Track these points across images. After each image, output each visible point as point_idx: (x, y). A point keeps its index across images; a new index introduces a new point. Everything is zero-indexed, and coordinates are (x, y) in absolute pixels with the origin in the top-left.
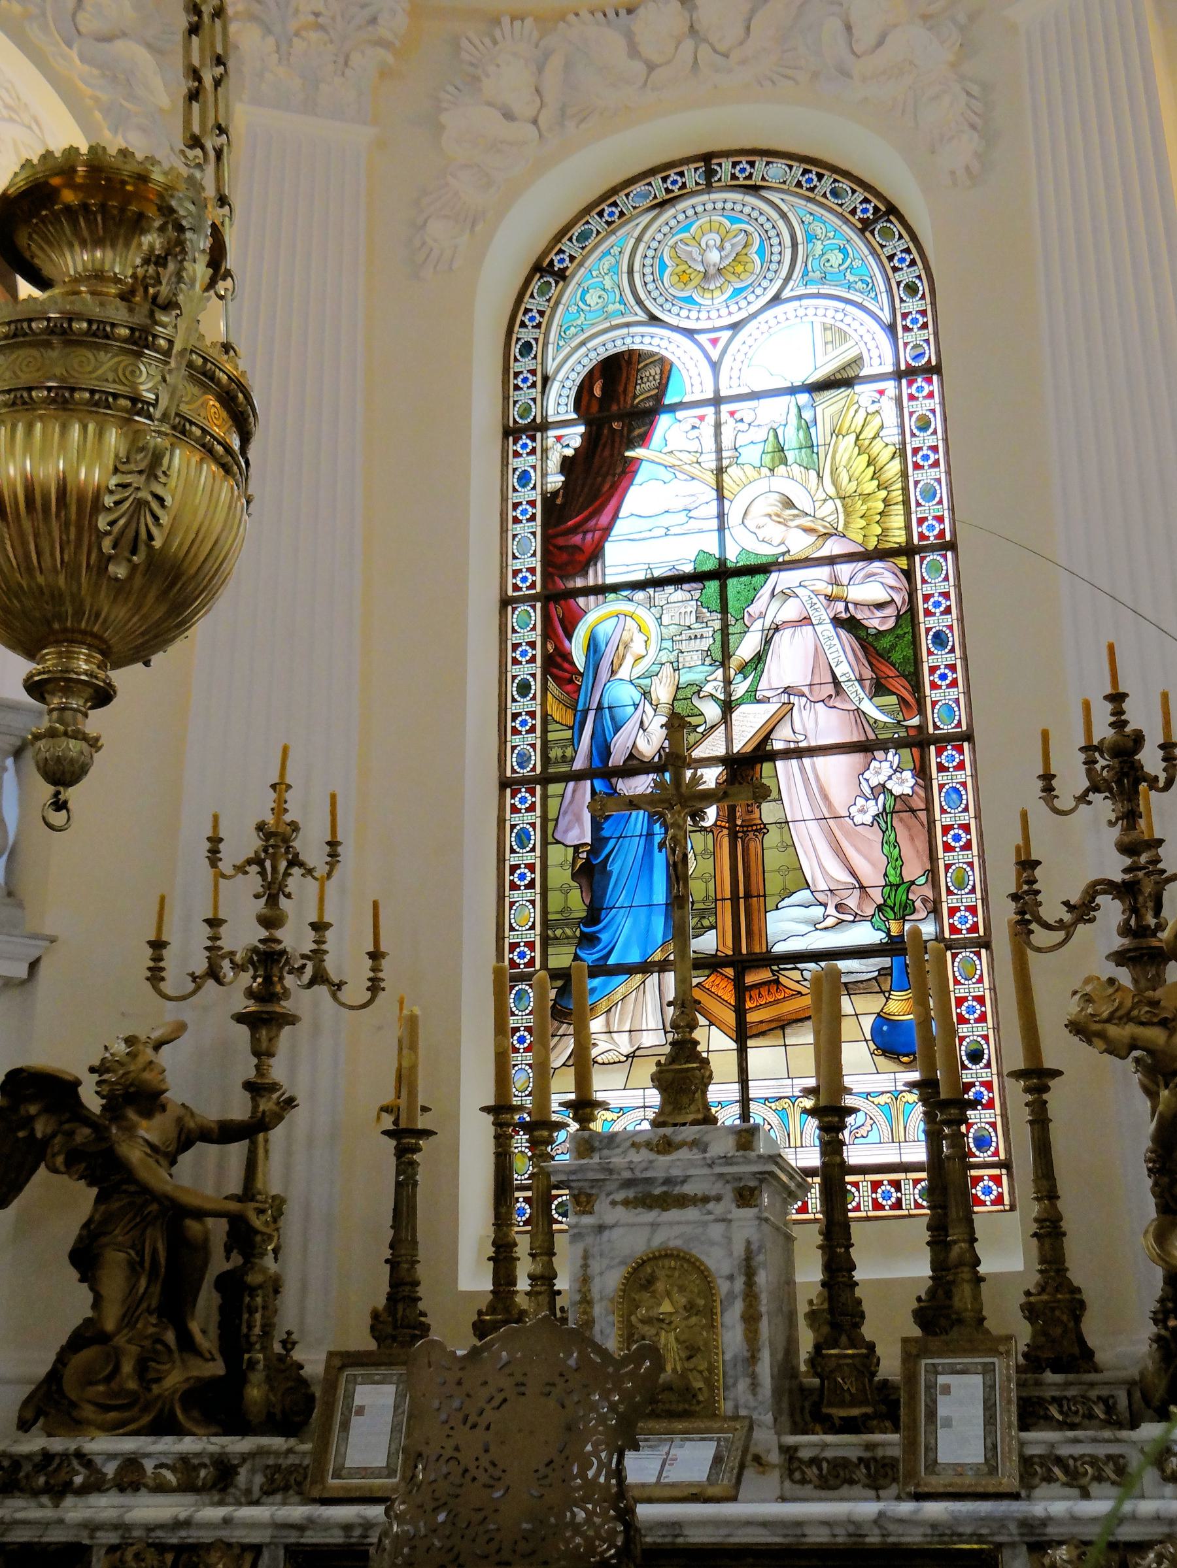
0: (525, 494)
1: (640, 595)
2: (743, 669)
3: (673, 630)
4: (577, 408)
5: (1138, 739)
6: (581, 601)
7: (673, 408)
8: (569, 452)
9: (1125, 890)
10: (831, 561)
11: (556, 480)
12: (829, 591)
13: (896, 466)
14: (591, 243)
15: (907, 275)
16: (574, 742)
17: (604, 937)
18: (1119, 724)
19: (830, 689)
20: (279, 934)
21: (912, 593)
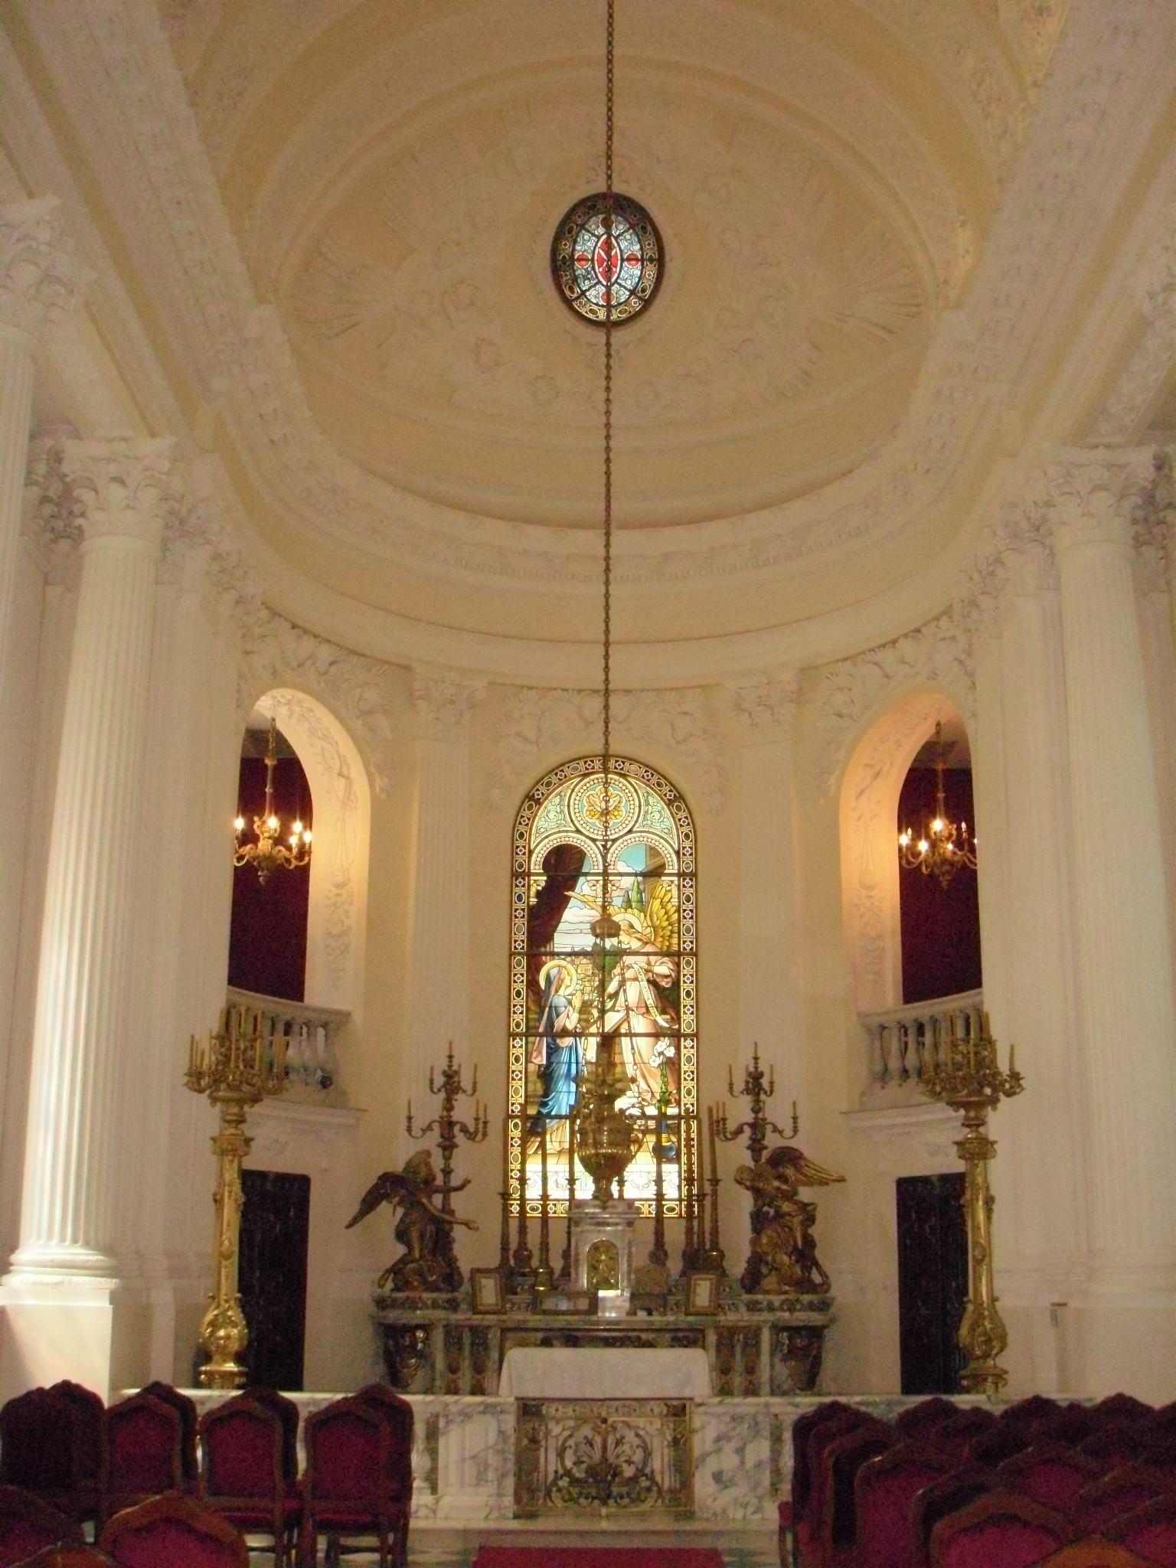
0: (520, 905)
1: (569, 959)
2: (611, 997)
3: (582, 976)
4: (543, 869)
5: (761, 1075)
6: (544, 958)
7: (586, 874)
8: (540, 888)
9: (754, 1126)
10: (648, 954)
11: (533, 901)
12: (646, 967)
13: (676, 916)
14: (551, 788)
15: (686, 830)
16: (539, 1020)
17: (550, 1103)
18: (756, 1068)
19: (644, 1010)
20: (452, 1113)
21: (679, 973)
